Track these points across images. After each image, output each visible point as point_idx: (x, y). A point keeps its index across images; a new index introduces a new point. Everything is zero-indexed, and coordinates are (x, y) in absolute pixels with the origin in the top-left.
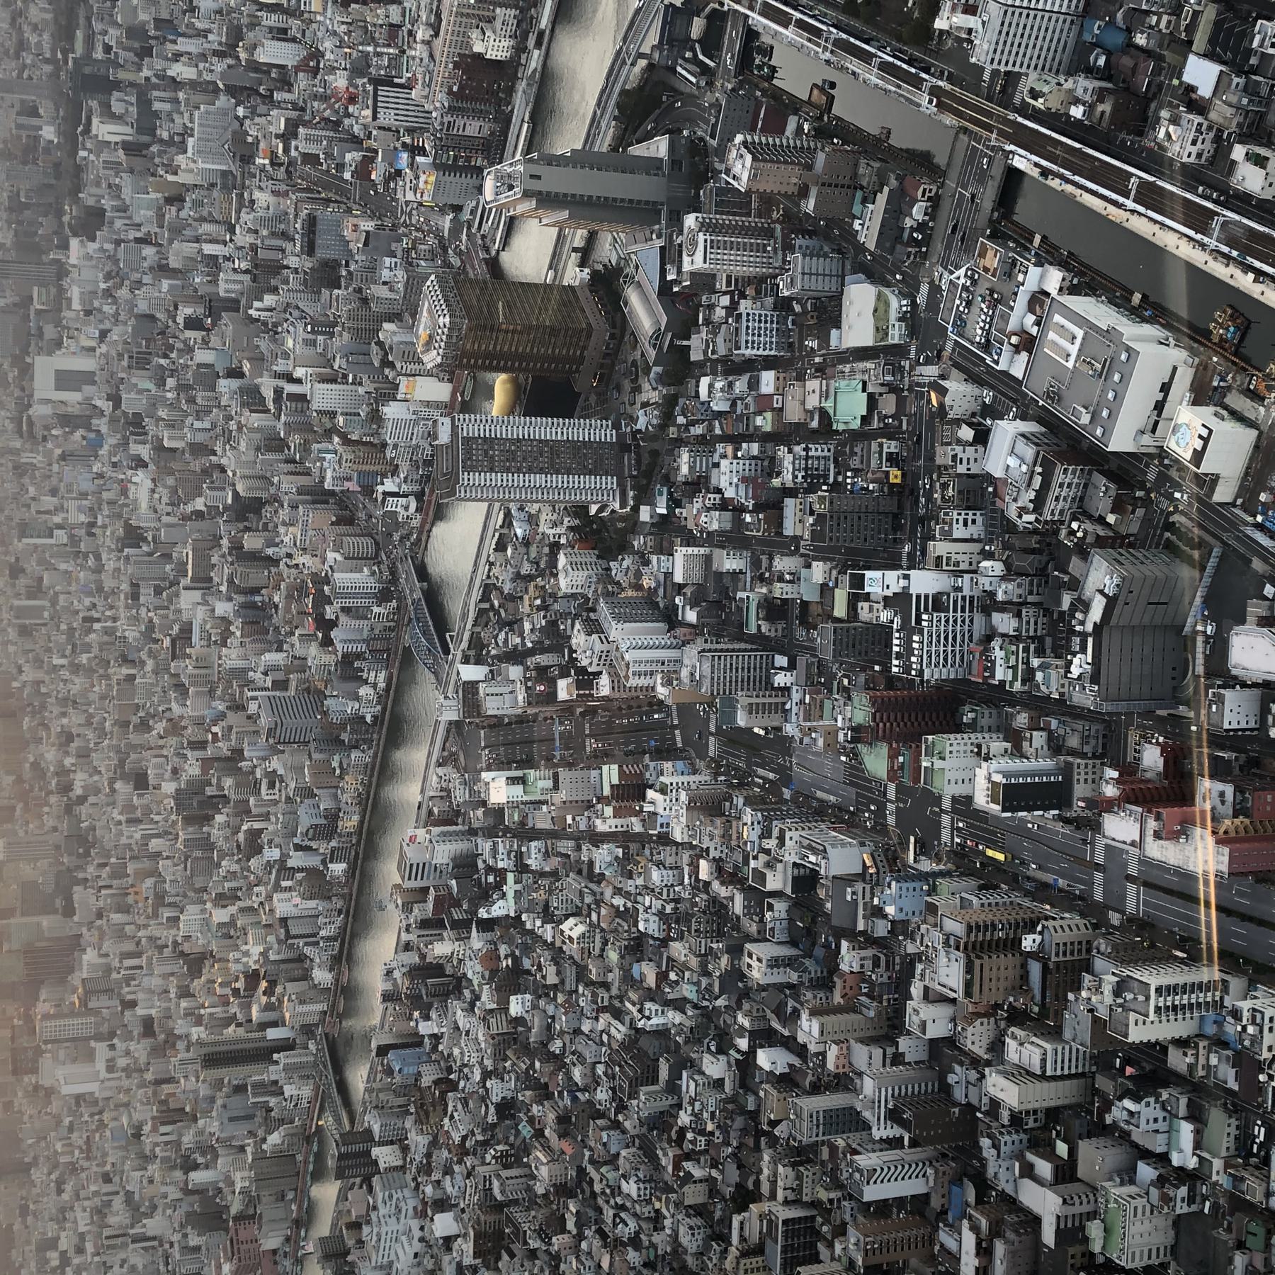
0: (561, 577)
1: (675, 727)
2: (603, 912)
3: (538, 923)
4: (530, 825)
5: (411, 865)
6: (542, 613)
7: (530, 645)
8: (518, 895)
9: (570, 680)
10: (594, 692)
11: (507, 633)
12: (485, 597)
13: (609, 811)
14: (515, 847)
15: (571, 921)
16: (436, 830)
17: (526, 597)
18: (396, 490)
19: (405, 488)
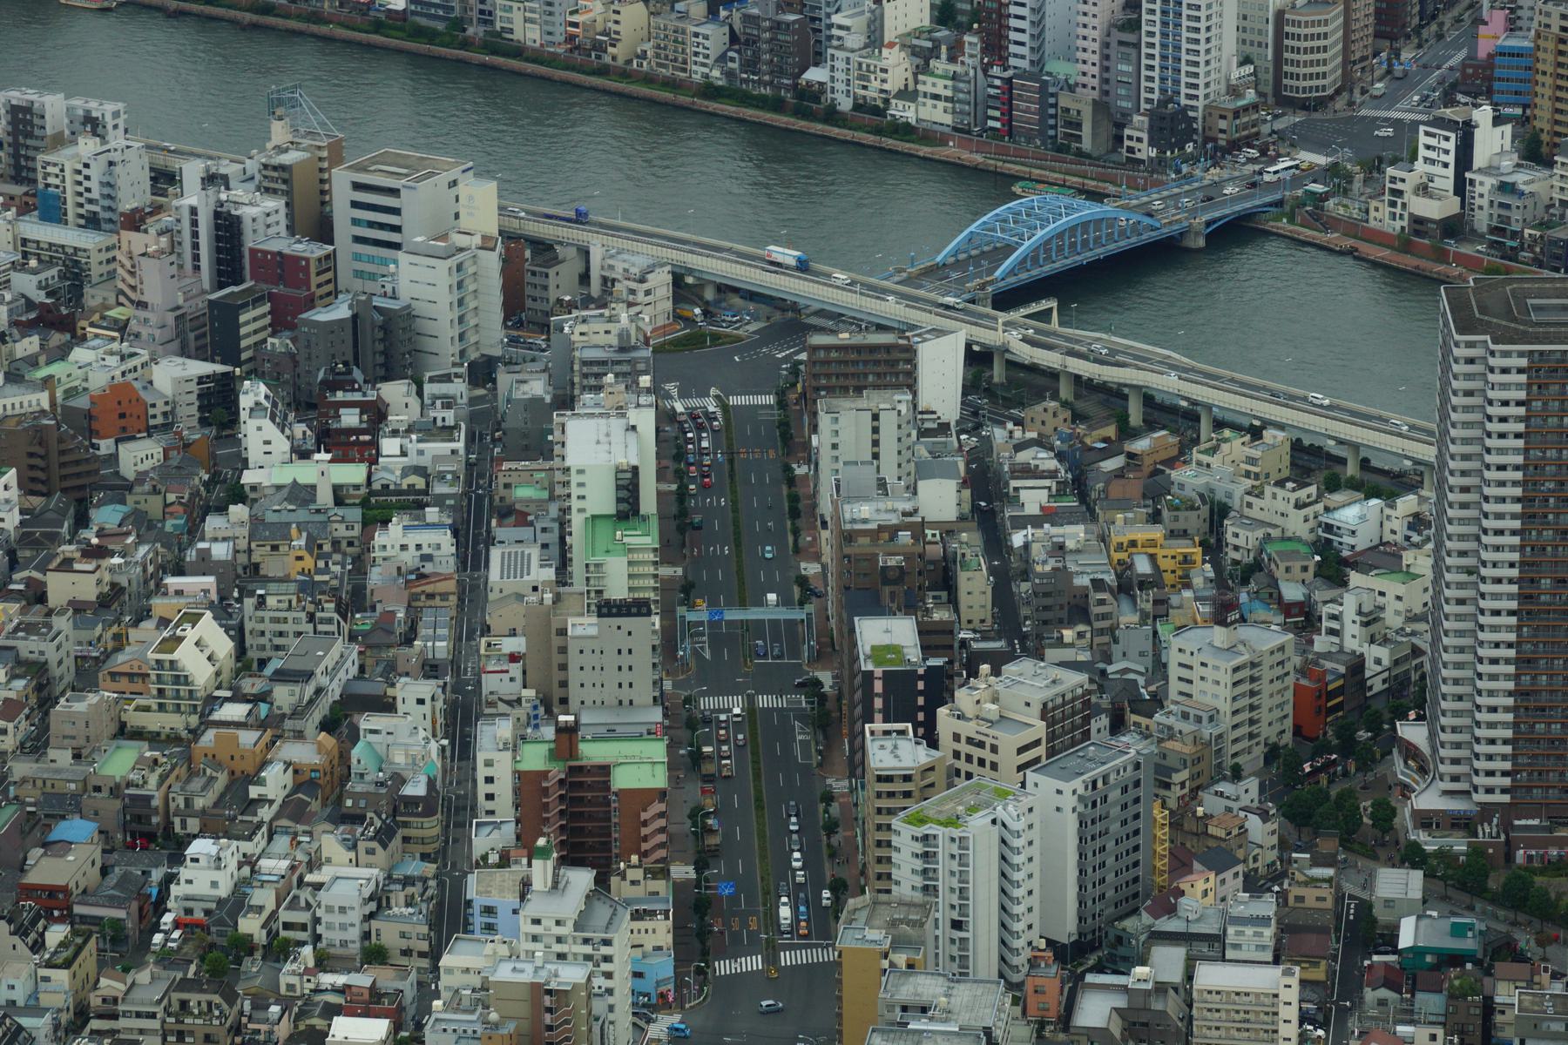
0: (1219, 635)
1: (771, 960)
2: (248, 738)
3: (220, 551)
4: (500, 533)
5: (394, 192)
6: (1110, 578)
7: (1018, 539)
8: (301, 494)
9: (914, 654)
10: (879, 726)
11: (1052, 474)
12: (1160, 412)
13: (535, 758)
14: (440, 489)
15: (223, 645)
16: (492, 262)
17: (1157, 532)
18: (1480, 158)
19: (1484, 186)
